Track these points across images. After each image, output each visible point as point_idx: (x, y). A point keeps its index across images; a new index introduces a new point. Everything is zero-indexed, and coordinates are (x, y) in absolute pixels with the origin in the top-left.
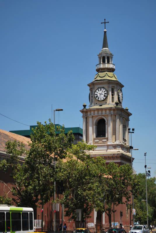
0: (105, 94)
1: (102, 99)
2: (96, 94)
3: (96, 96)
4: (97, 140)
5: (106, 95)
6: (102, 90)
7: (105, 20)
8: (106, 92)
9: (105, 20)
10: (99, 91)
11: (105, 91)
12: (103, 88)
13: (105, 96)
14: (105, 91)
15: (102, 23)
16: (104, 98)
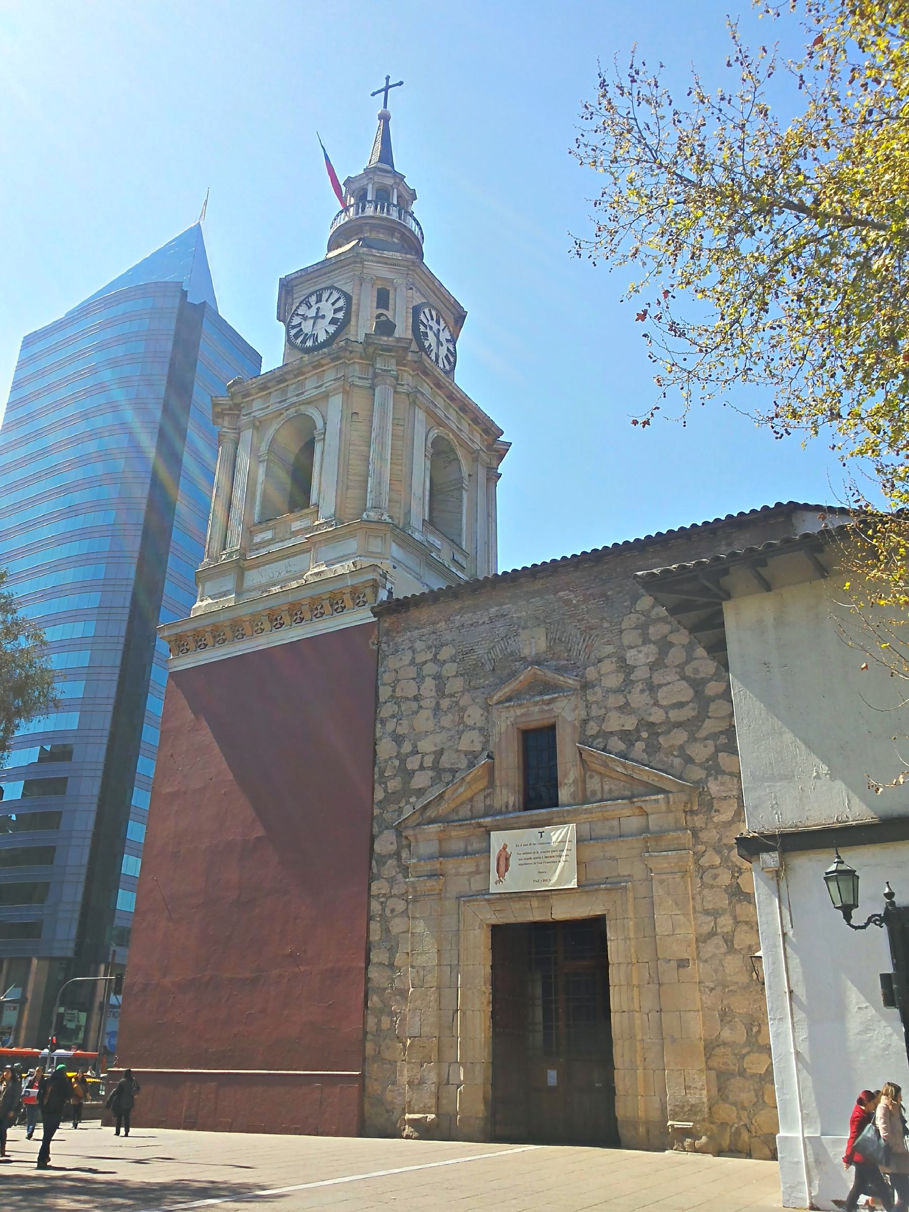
0: (336, 311)
1: (322, 337)
2: (294, 327)
3: (293, 332)
4: (268, 535)
5: (340, 315)
6: (325, 295)
7: (388, 78)
8: (341, 303)
9: (388, 78)
10: (310, 307)
11: (339, 298)
12: (332, 287)
13: (333, 321)
14: (339, 298)
15: (373, 95)
16: (332, 329)
